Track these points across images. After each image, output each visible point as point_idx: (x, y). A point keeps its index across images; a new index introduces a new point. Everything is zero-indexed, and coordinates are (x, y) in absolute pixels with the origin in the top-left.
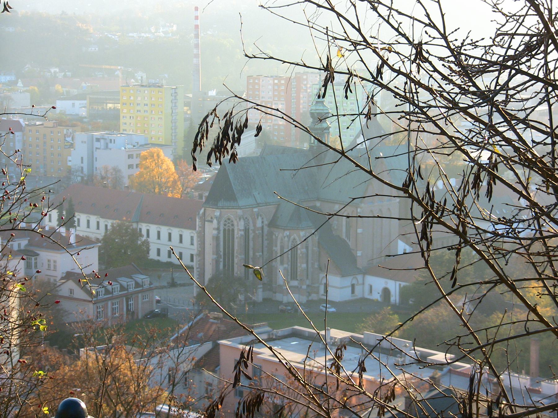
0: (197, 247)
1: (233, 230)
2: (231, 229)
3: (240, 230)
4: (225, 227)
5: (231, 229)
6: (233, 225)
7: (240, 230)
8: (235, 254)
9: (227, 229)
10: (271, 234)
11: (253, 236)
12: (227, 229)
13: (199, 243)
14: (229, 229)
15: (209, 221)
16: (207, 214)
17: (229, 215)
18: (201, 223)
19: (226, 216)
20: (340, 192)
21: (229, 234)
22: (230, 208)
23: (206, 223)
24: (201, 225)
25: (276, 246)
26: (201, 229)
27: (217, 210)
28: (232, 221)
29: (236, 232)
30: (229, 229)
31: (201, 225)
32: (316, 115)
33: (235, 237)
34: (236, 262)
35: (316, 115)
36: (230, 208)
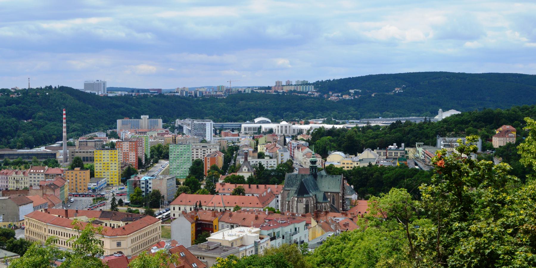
29: (309, 205)
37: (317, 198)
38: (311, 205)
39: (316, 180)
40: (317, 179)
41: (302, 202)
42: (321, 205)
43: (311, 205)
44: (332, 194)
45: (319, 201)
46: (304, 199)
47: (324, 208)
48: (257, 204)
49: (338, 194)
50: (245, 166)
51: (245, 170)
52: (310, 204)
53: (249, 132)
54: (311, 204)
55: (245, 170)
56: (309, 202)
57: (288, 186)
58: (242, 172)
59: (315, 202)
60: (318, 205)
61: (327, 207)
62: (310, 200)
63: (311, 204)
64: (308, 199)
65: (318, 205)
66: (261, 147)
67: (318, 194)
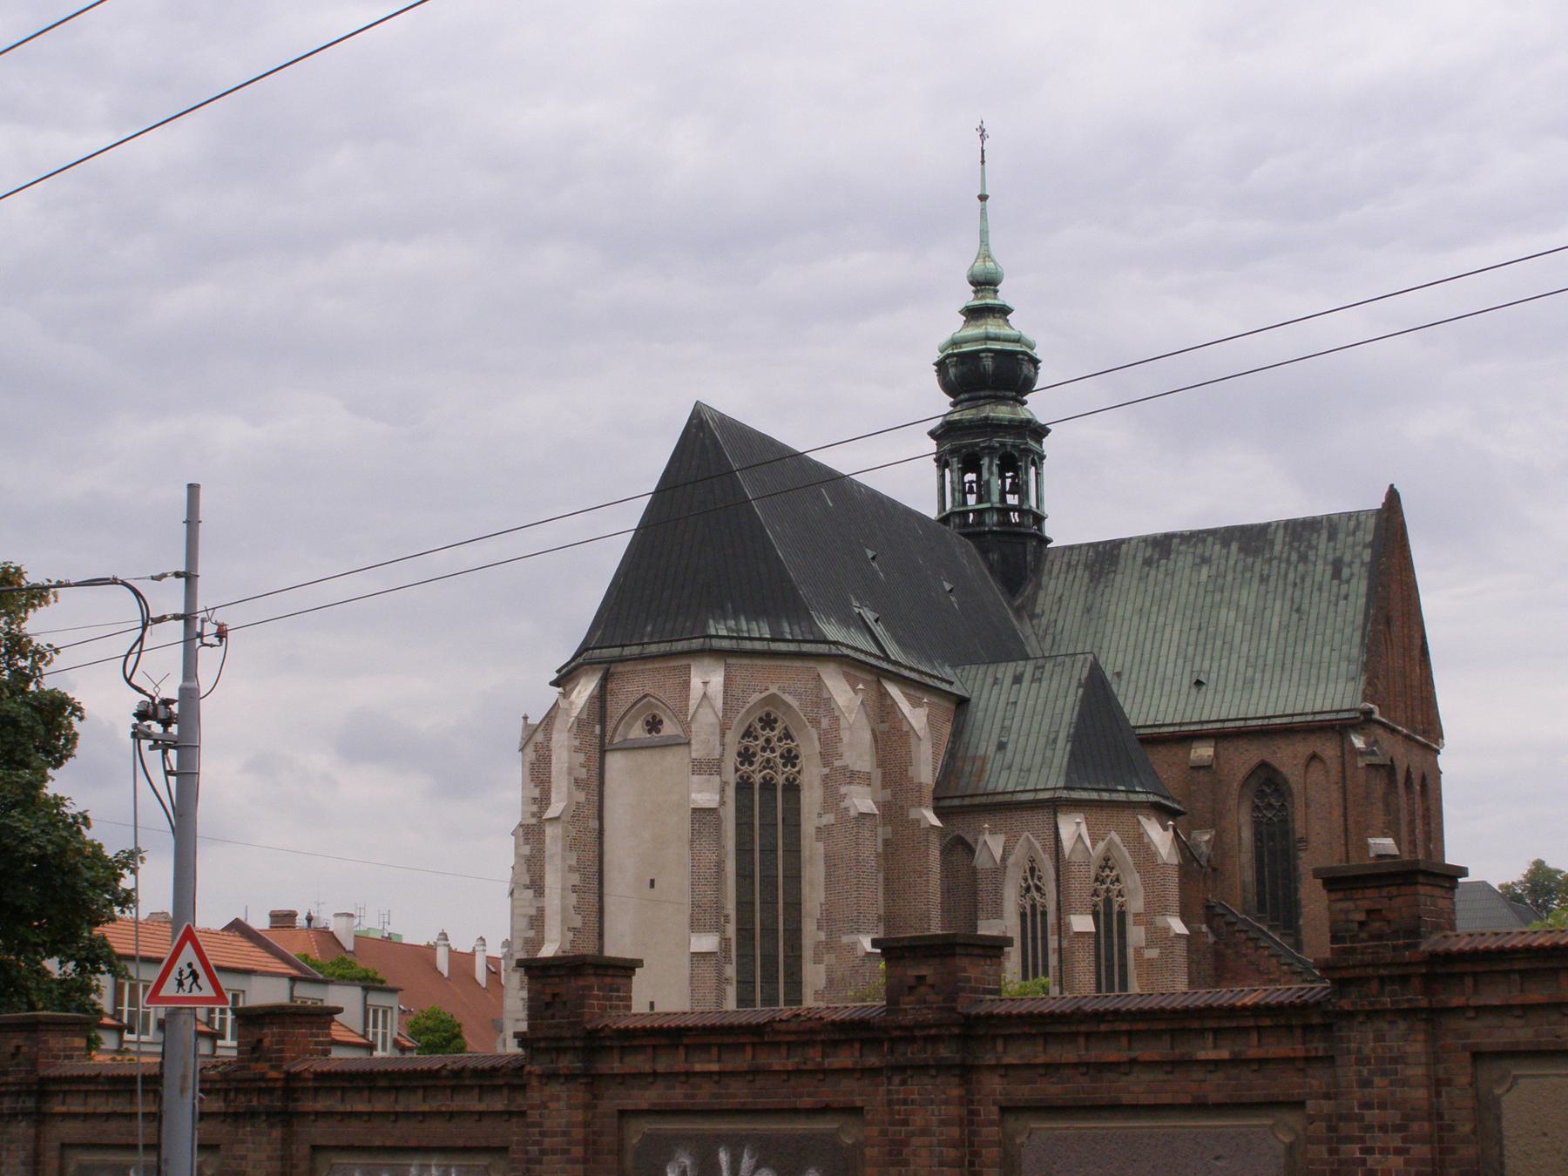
0: (564, 909)
1: (792, 788)
2: (780, 780)
3: (852, 776)
5: (780, 780)
6: (790, 758)
7: (852, 776)
8: (811, 934)
9: (757, 779)
10: (959, 848)
11: (886, 842)
12: (757, 779)
13: (575, 879)
14: (768, 785)
16: (617, 707)
17: (773, 689)
18: (581, 758)
19: (756, 697)
20: (1199, 683)
23: (615, 762)
24: (582, 773)
25: (998, 913)
26: (581, 796)
27: (707, 662)
28: (787, 736)
29: (811, 798)
30: (768, 785)
31: (583, 774)
32: (988, 363)
33: (809, 824)
34: (821, 982)
35: (988, 363)
36: (782, 647)
38: (832, 799)
39: (1027, 611)
40: (1044, 601)
41: (667, 745)
42: (1029, 838)
43: (832, 799)
44: (1245, 757)
46: (707, 680)
47: (1081, 886)
49: (1328, 749)
52: (811, 776)
54: (838, 777)
56: (809, 746)
60: (992, 844)
62: (823, 702)
63: (838, 777)
65: (992, 844)
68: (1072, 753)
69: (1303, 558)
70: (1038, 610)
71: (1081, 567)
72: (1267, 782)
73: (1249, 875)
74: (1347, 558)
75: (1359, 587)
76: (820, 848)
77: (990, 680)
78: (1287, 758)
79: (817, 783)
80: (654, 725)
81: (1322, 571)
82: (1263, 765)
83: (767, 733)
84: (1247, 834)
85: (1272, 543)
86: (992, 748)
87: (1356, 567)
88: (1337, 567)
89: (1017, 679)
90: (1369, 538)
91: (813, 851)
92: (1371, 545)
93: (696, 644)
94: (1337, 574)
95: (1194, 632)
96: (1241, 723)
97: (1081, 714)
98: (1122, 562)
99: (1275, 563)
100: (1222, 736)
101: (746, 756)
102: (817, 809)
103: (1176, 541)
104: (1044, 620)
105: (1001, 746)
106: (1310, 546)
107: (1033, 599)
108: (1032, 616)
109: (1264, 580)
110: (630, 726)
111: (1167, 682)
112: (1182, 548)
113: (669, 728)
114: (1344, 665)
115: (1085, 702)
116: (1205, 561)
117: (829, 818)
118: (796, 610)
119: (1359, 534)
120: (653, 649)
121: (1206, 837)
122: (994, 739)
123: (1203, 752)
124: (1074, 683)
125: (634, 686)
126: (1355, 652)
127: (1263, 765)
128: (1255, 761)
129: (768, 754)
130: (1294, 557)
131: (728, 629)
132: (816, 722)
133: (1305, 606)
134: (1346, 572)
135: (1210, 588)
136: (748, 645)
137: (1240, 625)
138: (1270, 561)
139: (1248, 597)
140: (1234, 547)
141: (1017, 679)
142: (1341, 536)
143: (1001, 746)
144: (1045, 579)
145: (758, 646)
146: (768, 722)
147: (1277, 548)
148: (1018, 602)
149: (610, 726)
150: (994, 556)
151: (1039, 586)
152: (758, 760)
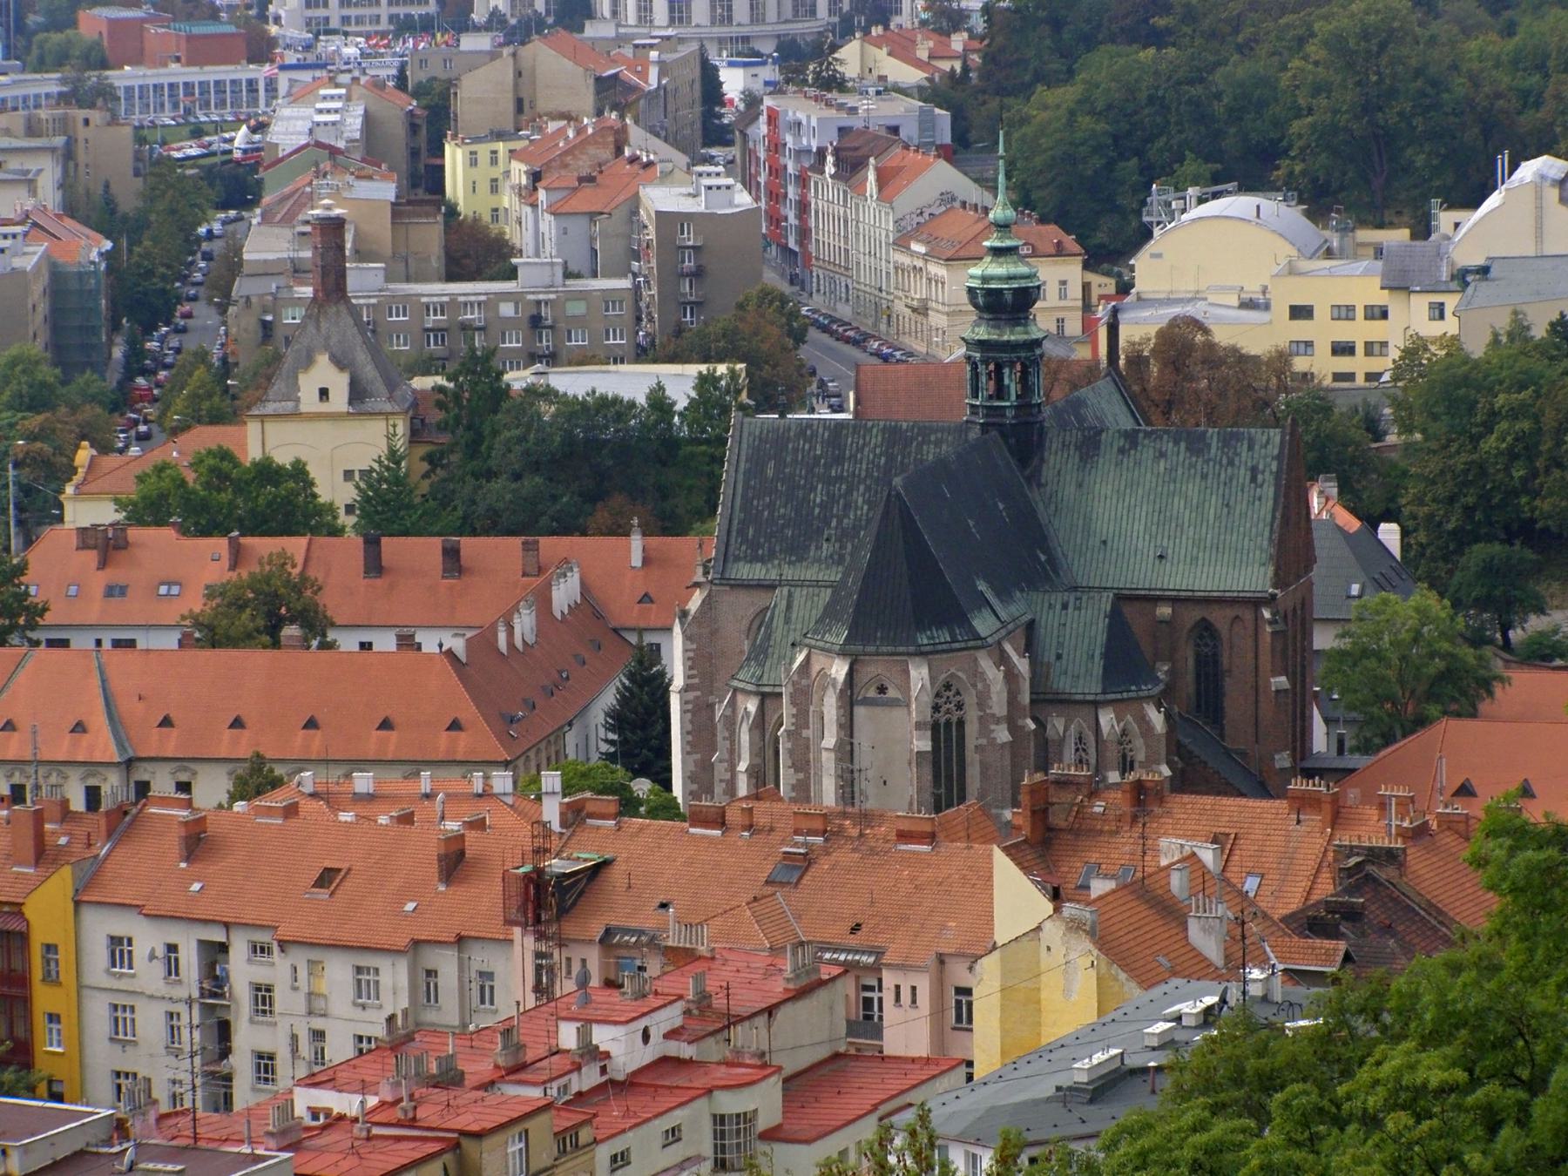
1: (961, 723)
2: (954, 719)
4: (936, 715)
6: (960, 706)
12: (943, 720)
15: (867, 702)
17: (953, 670)
19: (944, 676)
21: (948, 739)
22: (957, 645)
23: (860, 712)
28: (958, 693)
29: (971, 729)
30: (948, 724)
32: (1008, 297)
35: (1008, 297)
36: (957, 645)
37: (1050, 656)
38: (984, 730)
39: (1034, 479)
40: (1048, 473)
41: (894, 703)
42: (1080, 722)
43: (984, 730)
45: (1063, 684)
46: (919, 674)
47: (1112, 754)
48: (455, 726)
49: (1248, 615)
50: (323, 360)
51: (324, 393)
52: (972, 716)
53: (352, 12)
54: (985, 721)
55: (324, 393)
56: (970, 699)
57: (754, 545)
58: (295, 415)
59: (1025, 698)
60: (1057, 724)
61: (1139, 743)
62: (977, 674)
63: (985, 721)
64: (954, 667)
65: (1057, 724)
66: (473, 161)
67: (1049, 621)
68: (1105, 668)
69: (1231, 463)
70: (1043, 481)
71: (1072, 447)
72: (1205, 629)
73: (1191, 689)
74: (1261, 467)
75: (1269, 491)
76: (977, 757)
77: (1046, 605)
78: (1220, 618)
79: (975, 720)
80: (882, 690)
81: (1243, 474)
82: (1204, 619)
83: (947, 693)
84: (1191, 662)
85: (1209, 446)
86: (1053, 658)
87: (1267, 474)
88: (1254, 471)
89: (1065, 606)
90: (1276, 452)
91: (971, 756)
92: (1279, 458)
93: (912, 649)
94: (1254, 479)
95: (1156, 514)
96: (1190, 594)
97: (1109, 639)
98: (1102, 447)
99: (1211, 464)
100: (1175, 601)
101: (936, 708)
102: (975, 735)
103: (1141, 435)
104: (1048, 488)
105: (1059, 657)
106: (1236, 454)
107: (1038, 470)
108: (1039, 485)
109: (1204, 477)
110: (868, 690)
111: (1139, 553)
112: (1146, 442)
113: (892, 693)
114: (1258, 552)
115: (1110, 627)
116: (1162, 455)
117: (983, 741)
118: (963, 620)
119: (1270, 447)
120: (884, 649)
121: (1166, 668)
122: (1053, 652)
123: (1165, 611)
124: (1102, 616)
125: (873, 670)
126: (1265, 543)
127: (1204, 619)
128: (1198, 618)
129: (948, 706)
130: (1225, 461)
131: (929, 638)
132: (974, 686)
133: (1232, 503)
134: (1260, 477)
135: (1167, 479)
136: (940, 647)
137: (1187, 512)
138: (1209, 460)
139: (1193, 489)
140: (1183, 445)
141: (1065, 606)
142: (1257, 447)
143: (1059, 657)
144: (1046, 454)
145: (945, 647)
146: (948, 687)
147: (1213, 451)
148: (1027, 472)
149: (855, 691)
150: (1012, 441)
151: (1042, 460)
152: (943, 710)
